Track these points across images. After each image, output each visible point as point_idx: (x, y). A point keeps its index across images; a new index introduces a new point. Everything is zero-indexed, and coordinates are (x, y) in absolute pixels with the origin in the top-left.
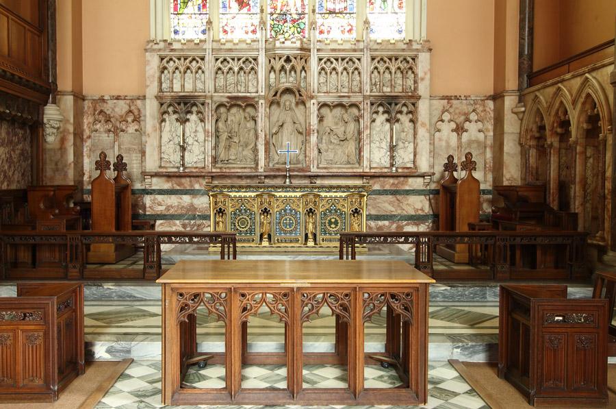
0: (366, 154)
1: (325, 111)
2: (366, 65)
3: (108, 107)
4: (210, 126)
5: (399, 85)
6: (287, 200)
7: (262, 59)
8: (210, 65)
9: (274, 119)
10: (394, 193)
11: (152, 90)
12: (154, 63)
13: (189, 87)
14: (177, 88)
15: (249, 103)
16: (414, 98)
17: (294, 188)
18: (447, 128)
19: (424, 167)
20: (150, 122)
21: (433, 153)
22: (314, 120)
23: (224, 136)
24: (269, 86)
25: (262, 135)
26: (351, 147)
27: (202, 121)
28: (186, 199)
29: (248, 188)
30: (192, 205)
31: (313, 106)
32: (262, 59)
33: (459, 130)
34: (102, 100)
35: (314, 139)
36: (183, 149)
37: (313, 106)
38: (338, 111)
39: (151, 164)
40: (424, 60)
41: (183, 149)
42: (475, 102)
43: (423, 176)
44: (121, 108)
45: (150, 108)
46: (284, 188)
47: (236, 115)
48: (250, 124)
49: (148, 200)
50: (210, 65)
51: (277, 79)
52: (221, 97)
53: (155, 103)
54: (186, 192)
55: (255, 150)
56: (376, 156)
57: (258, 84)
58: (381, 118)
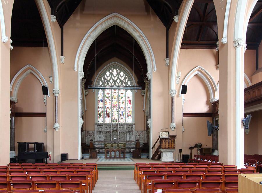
0: (126, 139)
1: (120, 133)
2: (126, 127)
3: (89, 132)
4: (104, 135)
5: (130, 129)
6: (115, 145)
7: (111, 126)
8: (104, 126)
9: (113, 134)
10: (130, 144)
11: (96, 130)
12: (96, 126)
13: (101, 130)
14: (99, 130)
15: (109, 132)
16: (132, 131)
17: (116, 143)
18: (137, 135)
19: (134, 141)
20: (96, 135)
21: (135, 139)
22: (119, 134)
23: (106, 136)
24: (112, 129)
25: (111, 136)
26: (124, 138)
27: (103, 134)
28: (101, 145)
29: (110, 143)
30: (101, 146)
31: (118, 132)
32: (111, 126)
33: (139, 135)
34: (89, 131)
35: (119, 137)
36: (100, 138)
37: (118, 132)
38: (122, 133)
39: (96, 140)
40: (134, 126)
41: (100, 138)
42: (141, 132)
43: (134, 142)
44: (91, 132)
45: (96, 132)
46: (114, 143)
47: (108, 133)
48: (110, 135)
49: (95, 145)
50: (104, 126)
51: (114, 128)
52: (106, 131)
53: (96, 132)
54: (100, 144)
55: (110, 138)
56: (128, 139)
57: (111, 129)
58: (128, 134)
